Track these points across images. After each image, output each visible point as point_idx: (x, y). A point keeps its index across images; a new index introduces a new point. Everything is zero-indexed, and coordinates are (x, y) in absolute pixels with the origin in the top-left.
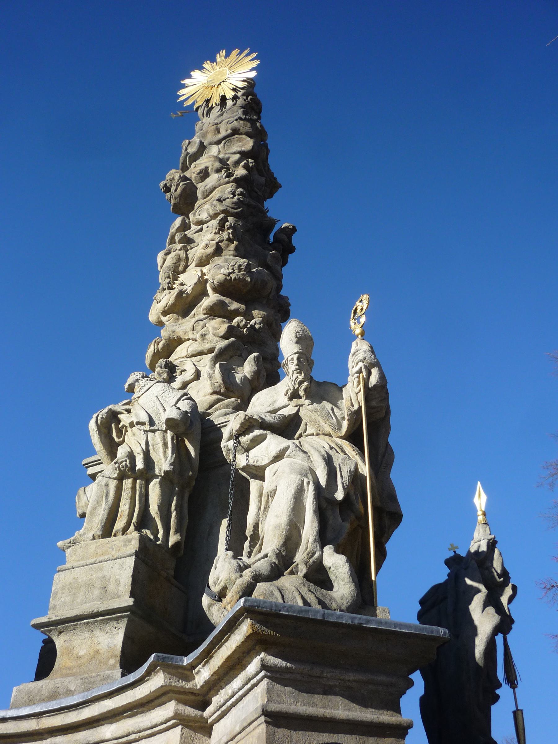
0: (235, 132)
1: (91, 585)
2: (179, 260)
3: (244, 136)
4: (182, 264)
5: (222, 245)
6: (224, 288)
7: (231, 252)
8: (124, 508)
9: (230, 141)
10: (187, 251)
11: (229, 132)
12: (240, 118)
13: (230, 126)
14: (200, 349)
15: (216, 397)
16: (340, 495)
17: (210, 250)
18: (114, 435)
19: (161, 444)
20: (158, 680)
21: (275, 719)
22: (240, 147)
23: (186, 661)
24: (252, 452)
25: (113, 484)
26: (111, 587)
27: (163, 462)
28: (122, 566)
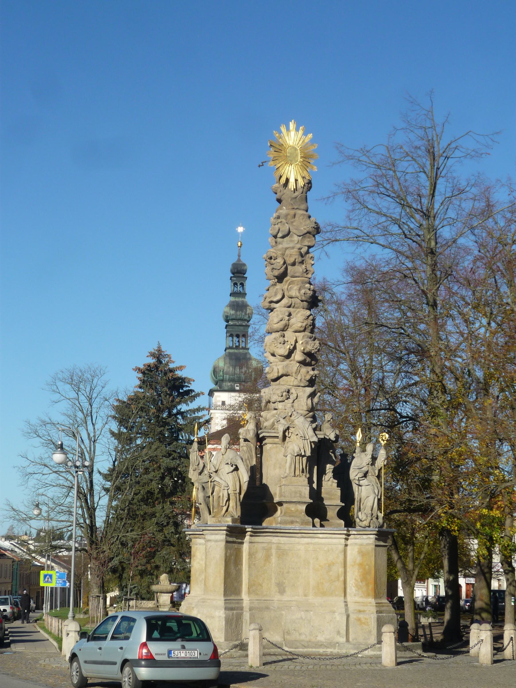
0: (309, 233)
1: (296, 492)
2: (286, 326)
3: (311, 236)
4: (286, 327)
5: (307, 326)
6: (309, 354)
7: (309, 331)
8: (297, 466)
9: (305, 237)
10: (289, 320)
11: (305, 231)
12: (314, 227)
13: (308, 229)
14: (299, 385)
15: (307, 412)
16: (379, 497)
17: (302, 329)
18: (287, 434)
19: (307, 445)
20: (345, 532)
21: (376, 546)
22: (309, 242)
23: (350, 529)
24: (361, 482)
25: (294, 457)
26: (303, 494)
27: (308, 453)
28: (305, 489)
